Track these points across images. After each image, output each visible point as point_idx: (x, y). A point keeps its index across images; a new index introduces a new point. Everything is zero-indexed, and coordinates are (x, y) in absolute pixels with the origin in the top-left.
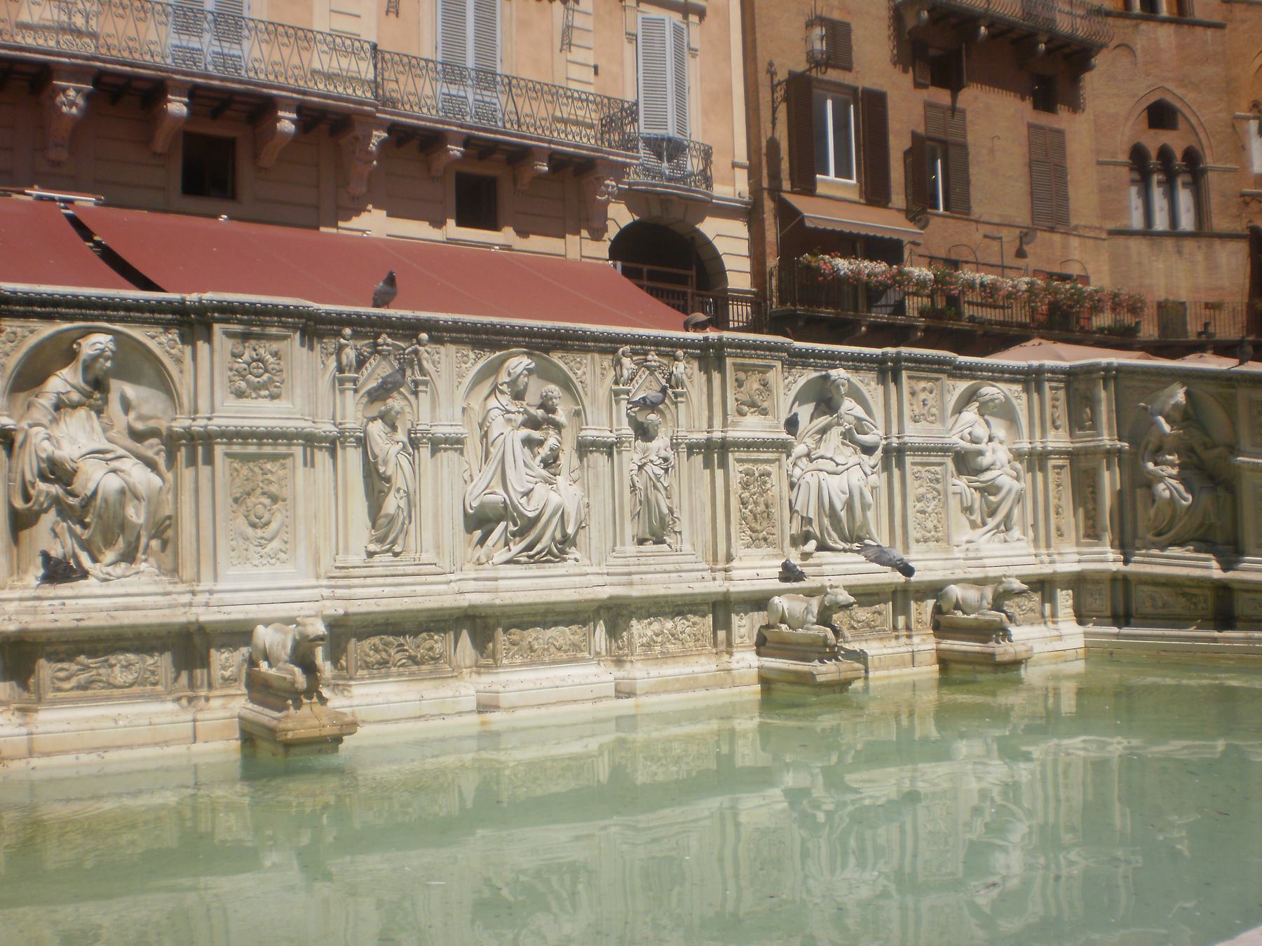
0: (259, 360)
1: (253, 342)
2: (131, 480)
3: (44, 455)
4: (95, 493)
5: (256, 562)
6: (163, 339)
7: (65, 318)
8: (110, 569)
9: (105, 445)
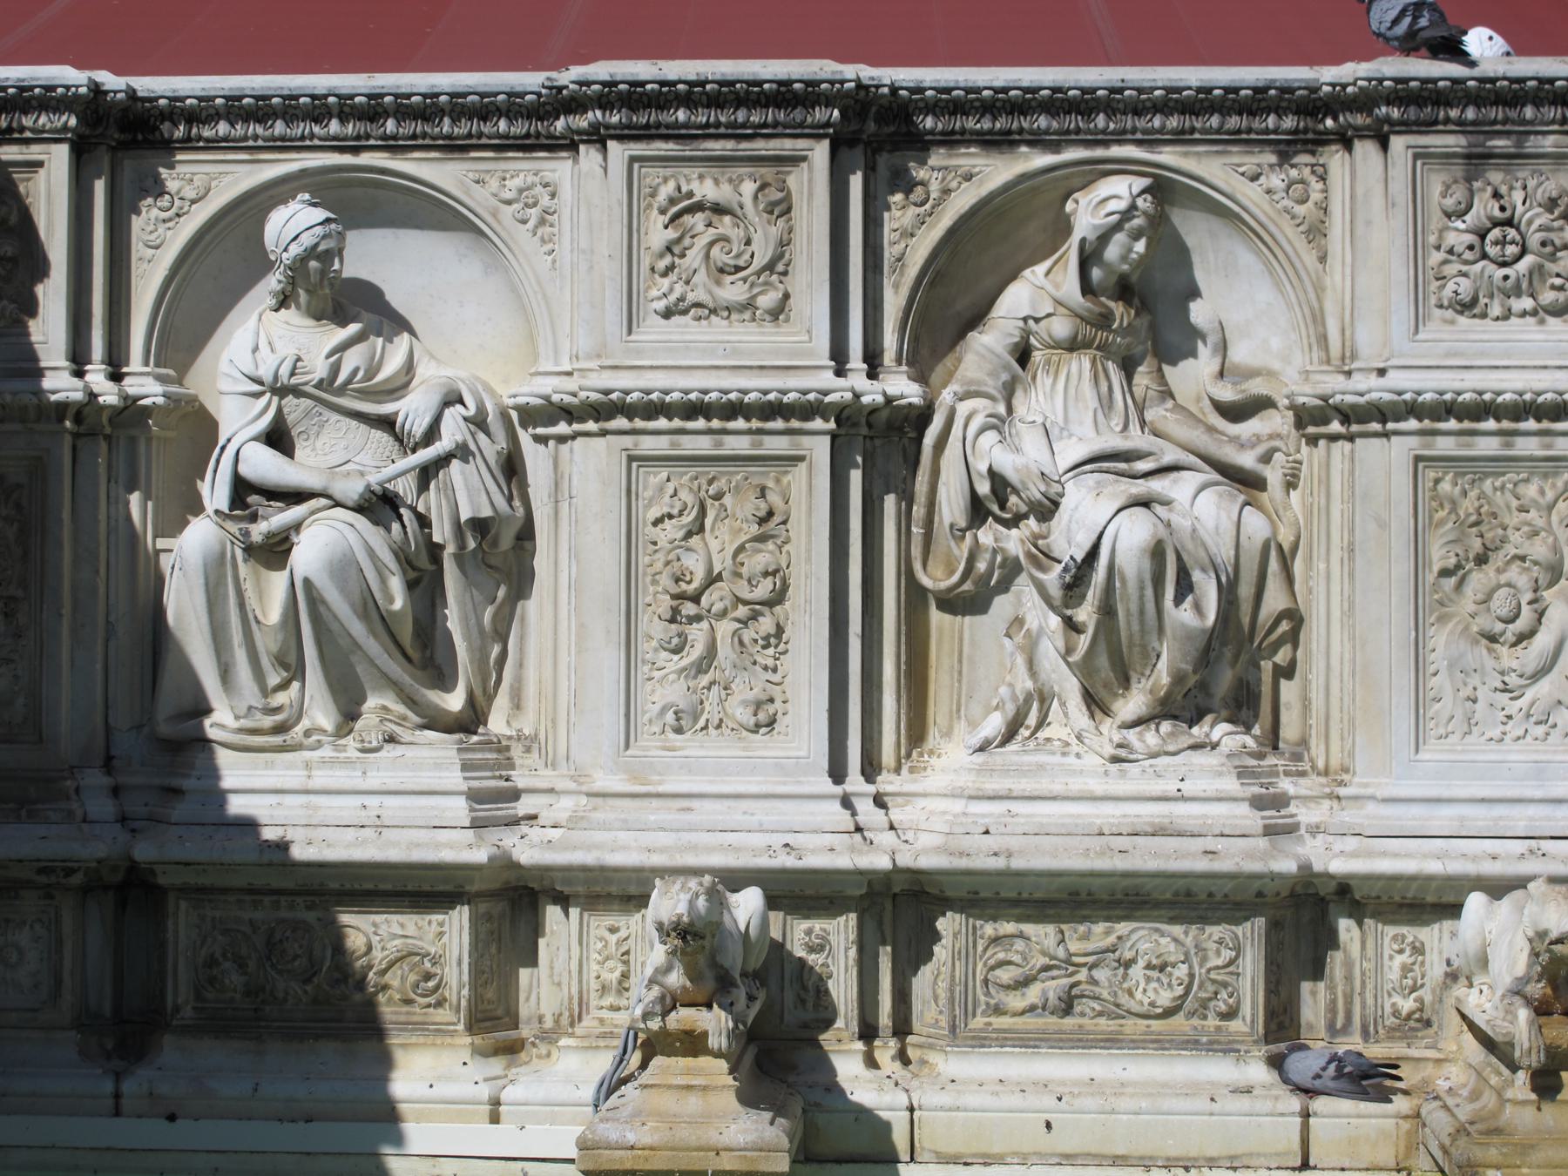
0: (1509, 223)
1: (1496, 177)
2: (1181, 522)
3: (983, 467)
4: (1093, 554)
5: (1496, 733)
6: (1276, 180)
7: (1039, 141)
8: (1132, 735)
9: (1137, 439)
